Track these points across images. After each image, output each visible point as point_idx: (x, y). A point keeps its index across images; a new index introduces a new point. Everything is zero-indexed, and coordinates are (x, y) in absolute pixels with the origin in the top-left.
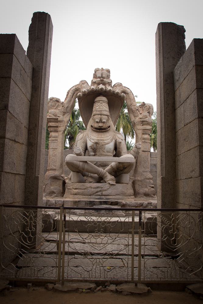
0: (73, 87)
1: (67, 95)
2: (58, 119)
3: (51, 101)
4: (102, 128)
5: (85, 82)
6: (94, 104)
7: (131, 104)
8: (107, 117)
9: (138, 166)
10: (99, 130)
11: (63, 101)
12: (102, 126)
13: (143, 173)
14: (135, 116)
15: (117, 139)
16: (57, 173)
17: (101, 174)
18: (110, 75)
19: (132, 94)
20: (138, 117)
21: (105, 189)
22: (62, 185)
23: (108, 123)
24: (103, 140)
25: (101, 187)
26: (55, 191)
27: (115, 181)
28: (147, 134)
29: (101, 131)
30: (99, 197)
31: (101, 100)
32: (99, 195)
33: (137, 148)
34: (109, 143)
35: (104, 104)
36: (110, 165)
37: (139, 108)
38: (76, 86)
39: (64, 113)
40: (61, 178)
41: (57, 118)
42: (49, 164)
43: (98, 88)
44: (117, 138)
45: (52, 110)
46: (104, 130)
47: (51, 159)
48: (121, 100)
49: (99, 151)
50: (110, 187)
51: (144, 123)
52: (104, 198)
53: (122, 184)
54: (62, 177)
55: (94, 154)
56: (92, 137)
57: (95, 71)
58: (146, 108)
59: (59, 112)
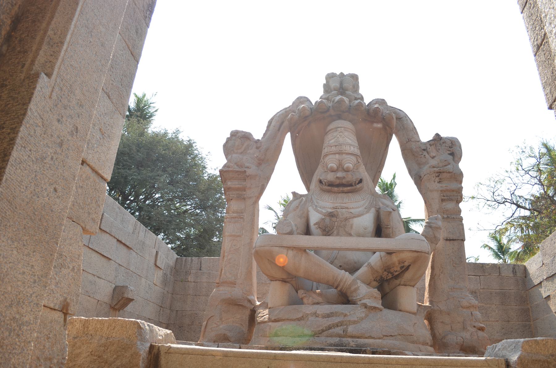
0: (281, 111)
2: (245, 172)
3: (234, 138)
4: (344, 181)
5: (305, 99)
7: (409, 140)
9: (436, 277)
10: (336, 189)
11: (260, 139)
12: (344, 178)
13: (451, 293)
14: (419, 164)
15: (380, 208)
16: (237, 292)
17: (342, 284)
18: (360, 85)
20: (428, 164)
21: (352, 319)
22: (248, 320)
24: (348, 208)
25: (343, 313)
26: (229, 334)
27: (381, 302)
28: (451, 200)
29: (341, 189)
30: (336, 340)
31: (339, 126)
32: (340, 336)
33: (430, 227)
34: (363, 214)
35: (346, 133)
36: (366, 264)
37: (429, 146)
38: (286, 109)
40: (246, 304)
42: (222, 270)
43: (333, 102)
44: (381, 205)
45: (234, 155)
46: (349, 188)
47: (225, 259)
50: (367, 316)
51: (444, 175)
52: (352, 344)
53: (401, 313)
54: (249, 301)
56: (322, 203)
57: (326, 78)
58: (444, 145)
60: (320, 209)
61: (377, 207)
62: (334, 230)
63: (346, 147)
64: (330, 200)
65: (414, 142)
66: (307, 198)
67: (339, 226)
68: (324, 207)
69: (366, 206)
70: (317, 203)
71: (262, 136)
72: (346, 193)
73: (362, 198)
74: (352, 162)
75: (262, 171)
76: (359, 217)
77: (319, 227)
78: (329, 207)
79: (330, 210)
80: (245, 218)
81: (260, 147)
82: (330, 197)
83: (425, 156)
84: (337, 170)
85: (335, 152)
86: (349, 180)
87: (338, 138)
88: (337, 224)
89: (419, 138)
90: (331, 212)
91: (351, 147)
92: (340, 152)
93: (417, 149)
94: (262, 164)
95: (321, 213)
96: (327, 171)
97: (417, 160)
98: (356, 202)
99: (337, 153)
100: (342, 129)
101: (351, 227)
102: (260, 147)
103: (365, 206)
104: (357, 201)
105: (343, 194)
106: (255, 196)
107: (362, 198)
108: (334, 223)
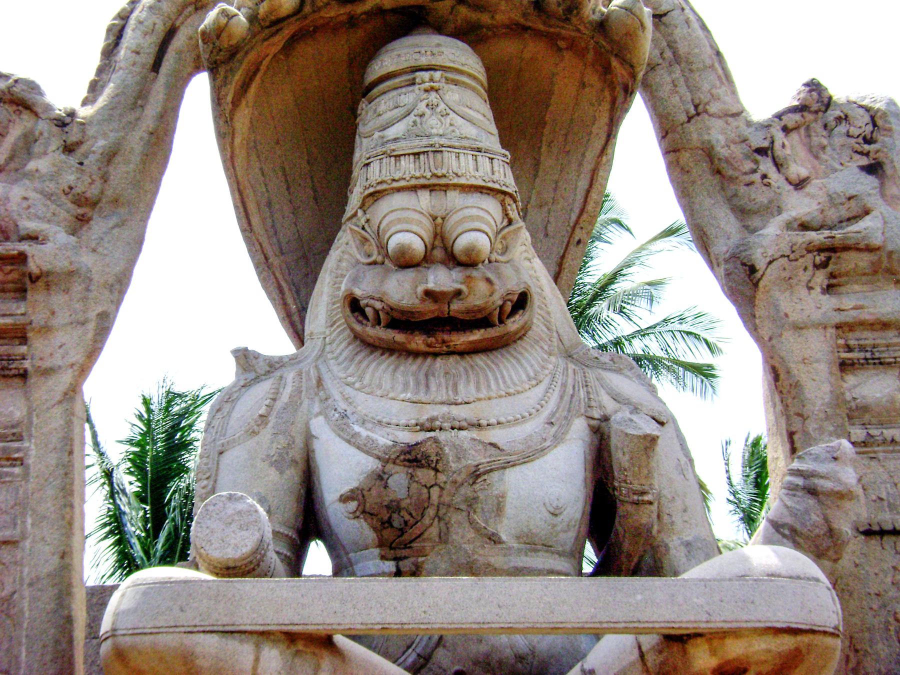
1: (109, 52)
2: (22, 258)
4: (456, 306)
6: (363, 104)
7: (698, 111)
8: (491, 206)
12: (458, 293)
14: (742, 212)
15: (606, 419)
19: (696, 25)
23: (507, 270)
34: (543, 451)
39: (80, 201)
41: (13, 247)
44: (610, 405)
46: (476, 336)
48: (607, 69)
49: (443, 538)
55: (390, 566)
59: (33, 195)
60: (364, 433)
61: (596, 416)
62: (427, 521)
63: (458, 157)
64: (400, 387)
65: (720, 117)
66: (300, 374)
67: (449, 506)
68: (380, 422)
69: (553, 414)
70: (346, 399)
71: (84, 93)
72: (462, 354)
73: (532, 374)
74: (488, 224)
75: (94, 251)
76: (528, 464)
77: (364, 512)
78: (403, 421)
79: (408, 437)
80: (30, 461)
81: (82, 143)
82: (399, 376)
83: (764, 176)
84: (425, 256)
85: (413, 182)
86: (478, 303)
87: (422, 115)
88: (440, 496)
89: (738, 102)
90: (410, 448)
91: (479, 158)
92: (435, 181)
93: (732, 147)
94: (88, 220)
95: (365, 448)
96: (383, 263)
97: (736, 195)
98: (509, 394)
99: (424, 187)
100: (437, 75)
101: (499, 509)
102: (79, 143)
103: (545, 413)
104: (511, 391)
105: (452, 359)
106: (72, 365)
107: (532, 374)
108: (425, 491)
